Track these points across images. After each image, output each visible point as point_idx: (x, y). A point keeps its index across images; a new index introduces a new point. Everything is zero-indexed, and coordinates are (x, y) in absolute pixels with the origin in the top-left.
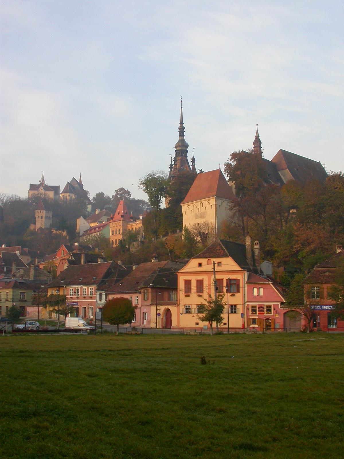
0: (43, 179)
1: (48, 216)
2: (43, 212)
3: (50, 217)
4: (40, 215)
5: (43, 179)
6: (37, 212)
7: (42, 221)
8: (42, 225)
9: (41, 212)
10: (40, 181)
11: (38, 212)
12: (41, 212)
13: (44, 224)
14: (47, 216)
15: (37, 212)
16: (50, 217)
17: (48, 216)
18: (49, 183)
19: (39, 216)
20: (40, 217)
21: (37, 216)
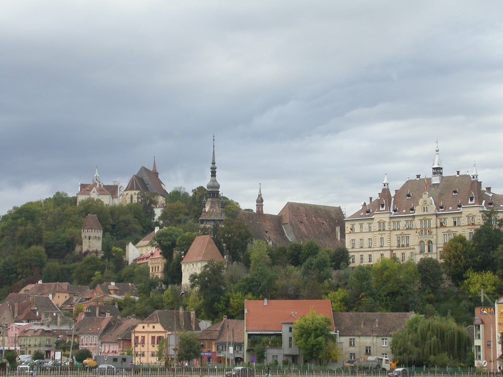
1: (97, 236)
2: (91, 231)
4: (87, 235)
6: (84, 231)
7: (89, 242)
11: (85, 231)
15: (84, 231)
17: (97, 236)
19: (85, 236)
20: (88, 237)
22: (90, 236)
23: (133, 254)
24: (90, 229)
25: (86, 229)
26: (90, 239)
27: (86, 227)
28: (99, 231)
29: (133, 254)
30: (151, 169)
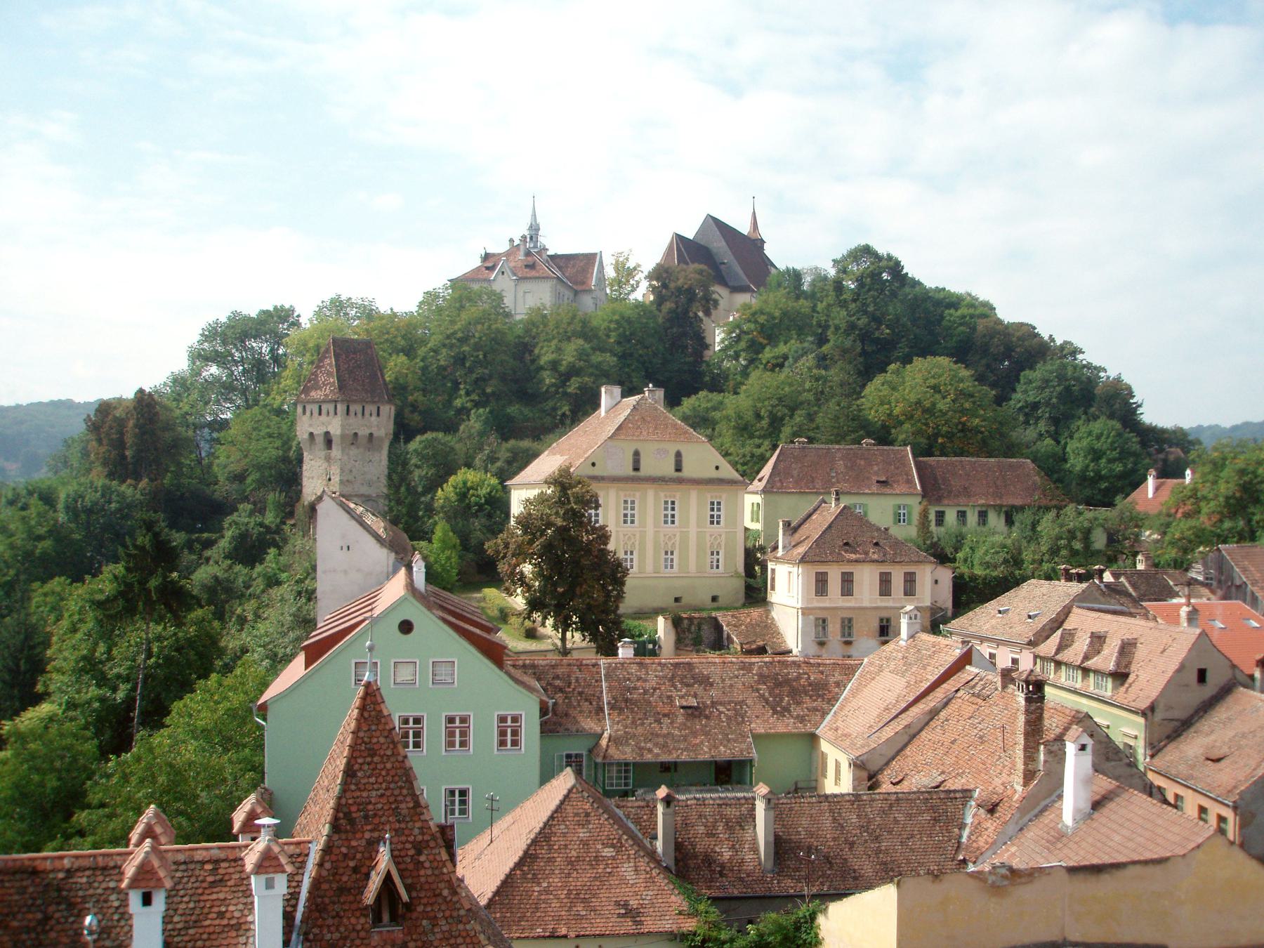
0: (535, 229)
1: (363, 432)
3: (371, 435)
4: (319, 431)
5: (535, 229)
6: (304, 412)
7: (328, 459)
8: (330, 480)
9: (320, 414)
10: (511, 241)
12: (320, 414)
13: (336, 479)
14: (356, 434)
15: (304, 412)
16: (371, 435)
18: (557, 242)
19: (311, 434)
20: (320, 440)
21: (306, 436)
22: (327, 433)
23: (346, 572)
24: (330, 401)
25: (314, 402)
26: (329, 442)
27: (313, 393)
28: (371, 408)
29: (346, 572)
30: (745, 228)
